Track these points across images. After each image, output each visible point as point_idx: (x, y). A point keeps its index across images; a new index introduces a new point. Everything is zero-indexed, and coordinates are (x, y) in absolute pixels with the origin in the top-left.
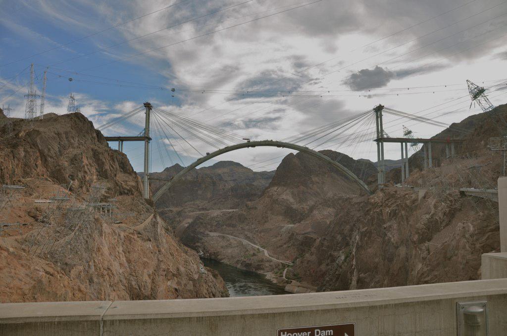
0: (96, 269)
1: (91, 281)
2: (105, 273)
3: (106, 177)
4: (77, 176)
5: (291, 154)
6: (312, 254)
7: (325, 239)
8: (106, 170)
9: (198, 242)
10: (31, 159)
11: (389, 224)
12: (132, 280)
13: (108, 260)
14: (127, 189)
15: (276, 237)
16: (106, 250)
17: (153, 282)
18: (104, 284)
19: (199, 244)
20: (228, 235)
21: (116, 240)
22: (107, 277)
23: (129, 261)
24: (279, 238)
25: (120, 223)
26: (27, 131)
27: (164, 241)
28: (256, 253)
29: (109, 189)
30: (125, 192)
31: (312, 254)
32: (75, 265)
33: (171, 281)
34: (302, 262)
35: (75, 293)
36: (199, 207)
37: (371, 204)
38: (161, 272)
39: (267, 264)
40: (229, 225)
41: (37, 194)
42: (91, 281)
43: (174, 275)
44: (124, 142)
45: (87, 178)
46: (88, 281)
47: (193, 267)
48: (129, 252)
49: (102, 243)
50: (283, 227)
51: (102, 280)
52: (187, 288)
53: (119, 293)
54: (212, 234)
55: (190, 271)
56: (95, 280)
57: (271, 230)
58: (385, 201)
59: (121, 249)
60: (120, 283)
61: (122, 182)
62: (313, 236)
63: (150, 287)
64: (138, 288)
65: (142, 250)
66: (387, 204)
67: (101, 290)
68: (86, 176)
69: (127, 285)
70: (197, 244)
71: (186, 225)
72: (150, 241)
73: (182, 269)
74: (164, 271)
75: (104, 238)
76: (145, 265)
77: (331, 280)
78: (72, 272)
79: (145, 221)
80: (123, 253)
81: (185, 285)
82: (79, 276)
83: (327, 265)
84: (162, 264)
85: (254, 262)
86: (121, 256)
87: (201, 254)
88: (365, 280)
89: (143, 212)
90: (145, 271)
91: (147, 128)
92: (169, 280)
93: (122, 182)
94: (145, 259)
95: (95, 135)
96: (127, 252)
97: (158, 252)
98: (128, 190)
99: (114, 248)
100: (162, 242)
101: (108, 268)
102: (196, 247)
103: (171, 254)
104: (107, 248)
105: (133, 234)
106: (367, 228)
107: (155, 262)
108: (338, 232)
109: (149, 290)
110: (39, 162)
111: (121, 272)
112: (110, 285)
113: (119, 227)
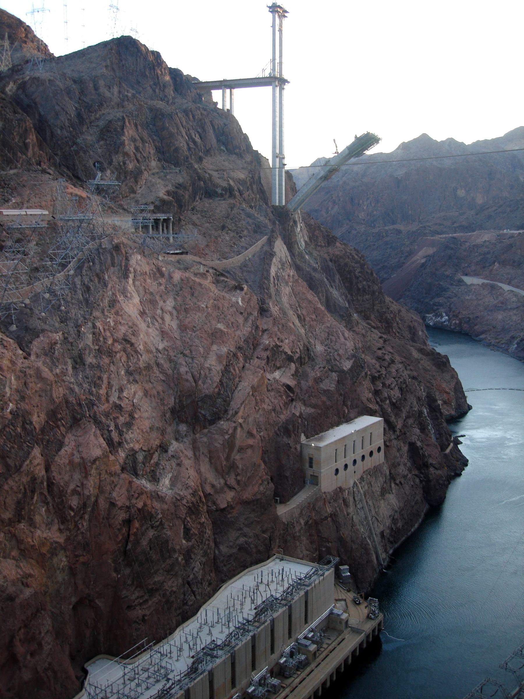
0: (96, 340)
1: (79, 361)
2: (118, 347)
3: (177, 165)
4: (110, 163)
8: (177, 150)
9: (438, 295)
10: (15, 134)
12: (181, 364)
13: (130, 324)
16: (131, 307)
17: (226, 370)
18: (112, 368)
19: (441, 300)
20: (500, 285)
21: (162, 287)
22: (121, 357)
23: (183, 328)
25: (182, 253)
26: (19, 82)
27: (286, 290)
29: (179, 186)
30: (216, 192)
32: (43, 331)
33: (283, 369)
35: (28, 381)
36: (453, 223)
38: (259, 352)
40: (503, 263)
41: (19, 200)
42: (79, 361)
43: (290, 359)
44: (236, 91)
45: (131, 166)
46: (69, 362)
47: (346, 345)
48: (186, 310)
49: (124, 292)
51: (106, 360)
52: (322, 386)
53: (148, 386)
54: (468, 280)
55: (336, 353)
56: (90, 360)
59: (170, 304)
60: (155, 368)
61: (215, 174)
63: (217, 379)
64: (191, 379)
65: (216, 307)
67: (100, 378)
68: (128, 162)
69: (170, 372)
70: (437, 300)
71: (423, 261)
72: (242, 289)
73: (319, 348)
74: (266, 350)
75: (130, 281)
76: (216, 336)
78: (35, 343)
79: (247, 249)
80: (175, 313)
81: (318, 380)
82: (49, 351)
84: (265, 336)
86: (167, 318)
87: (443, 320)
89: (245, 232)
90: (215, 347)
91: (276, 60)
92: (279, 368)
93: (215, 174)
94: (220, 326)
95: (167, 78)
96: (181, 310)
97: (256, 313)
99: (153, 302)
100: (278, 292)
101: (126, 340)
102: (434, 305)
103: (299, 317)
104: (136, 300)
105: (203, 275)
107: (246, 330)
109: (215, 385)
110: (32, 138)
111: (161, 347)
112: (129, 373)
113: (178, 262)
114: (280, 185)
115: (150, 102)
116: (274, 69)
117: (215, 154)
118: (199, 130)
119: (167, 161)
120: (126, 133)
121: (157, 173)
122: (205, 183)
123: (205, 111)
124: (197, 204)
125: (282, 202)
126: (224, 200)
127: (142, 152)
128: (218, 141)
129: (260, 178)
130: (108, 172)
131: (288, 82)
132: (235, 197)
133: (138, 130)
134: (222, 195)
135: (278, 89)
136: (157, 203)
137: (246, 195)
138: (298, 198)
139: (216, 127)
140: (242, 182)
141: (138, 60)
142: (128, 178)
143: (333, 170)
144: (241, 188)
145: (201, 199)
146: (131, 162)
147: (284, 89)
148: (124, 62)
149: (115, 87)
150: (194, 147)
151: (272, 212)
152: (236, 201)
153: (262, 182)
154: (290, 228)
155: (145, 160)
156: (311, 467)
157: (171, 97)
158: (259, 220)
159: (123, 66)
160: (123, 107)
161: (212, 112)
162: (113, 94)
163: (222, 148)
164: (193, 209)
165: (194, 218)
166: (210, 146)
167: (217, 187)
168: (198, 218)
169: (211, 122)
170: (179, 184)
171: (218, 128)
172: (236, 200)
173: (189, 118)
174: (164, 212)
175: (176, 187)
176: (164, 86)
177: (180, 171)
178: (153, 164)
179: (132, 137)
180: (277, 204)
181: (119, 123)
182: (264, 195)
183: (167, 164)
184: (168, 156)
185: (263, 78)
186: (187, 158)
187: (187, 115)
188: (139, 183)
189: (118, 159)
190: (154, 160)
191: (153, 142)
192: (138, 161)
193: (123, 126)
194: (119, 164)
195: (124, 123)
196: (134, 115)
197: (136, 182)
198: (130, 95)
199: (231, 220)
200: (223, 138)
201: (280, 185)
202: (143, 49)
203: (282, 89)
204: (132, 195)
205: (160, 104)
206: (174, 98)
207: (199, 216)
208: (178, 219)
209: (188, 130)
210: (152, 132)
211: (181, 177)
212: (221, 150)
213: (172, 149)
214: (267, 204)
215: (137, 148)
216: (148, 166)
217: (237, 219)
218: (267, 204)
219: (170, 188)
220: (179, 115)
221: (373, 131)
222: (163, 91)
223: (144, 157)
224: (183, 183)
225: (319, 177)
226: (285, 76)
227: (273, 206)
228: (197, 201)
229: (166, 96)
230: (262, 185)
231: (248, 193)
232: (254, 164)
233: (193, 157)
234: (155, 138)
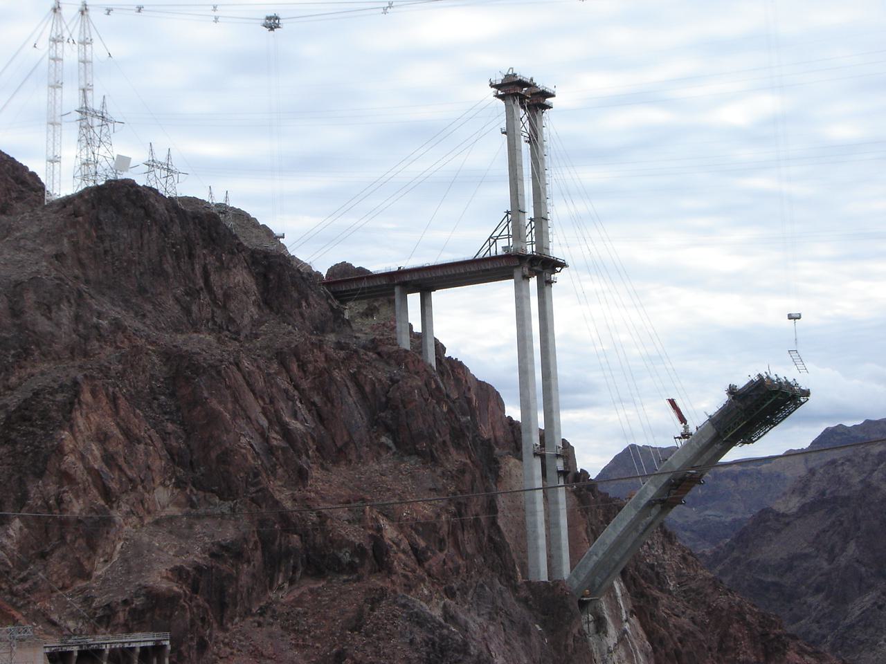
3: (227, 492)
4: (22, 501)
8: (225, 457)
14: (350, 544)
29: (221, 552)
30: (338, 561)
44: (437, 296)
45: (77, 508)
68: (68, 496)
93: (343, 513)
95: (241, 277)
98: (359, 551)
114: (551, 524)
115: (166, 338)
116: (517, 235)
117: (360, 457)
118: (317, 399)
119: (197, 485)
120: (81, 421)
121: (171, 519)
122: (304, 536)
123: (342, 349)
124: (283, 596)
125: (561, 571)
126: (359, 579)
127: (125, 466)
128: (375, 422)
129: (492, 508)
130: (17, 523)
131: (563, 265)
132: (391, 571)
133: (117, 413)
134: (352, 568)
135: (533, 282)
136: (138, 602)
137: (435, 561)
138: (595, 558)
139: (368, 389)
140: (428, 528)
141: (146, 235)
142: (69, 538)
143: (683, 480)
144: (422, 544)
145: (292, 582)
146: (77, 497)
147: (550, 283)
148: (107, 244)
149: (65, 306)
150: (284, 444)
151: (525, 601)
152: (393, 582)
153: (500, 523)
154: (571, 641)
155: (134, 488)
157: (246, 321)
158: (445, 632)
159: (106, 252)
160: (86, 354)
161: (362, 351)
162: (58, 325)
163: (383, 439)
164: (262, 612)
165: (259, 636)
166: (346, 438)
167: (340, 548)
168: (270, 636)
169: (354, 377)
170: (222, 547)
171: (373, 390)
172: (394, 578)
173: (288, 371)
174: (155, 628)
175: (213, 555)
176: (227, 296)
177: (232, 509)
178: (162, 495)
179: (99, 428)
180: (544, 577)
181: (60, 397)
182: (499, 553)
183: (201, 494)
184: (204, 470)
185: (492, 259)
186: (256, 475)
187: (283, 364)
188: (100, 551)
189: (41, 490)
190: (163, 484)
191: (164, 440)
192: (107, 494)
193: (72, 404)
194: (47, 503)
195: (77, 394)
196: (113, 373)
197: (92, 547)
198: (105, 323)
199: (367, 635)
200: (386, 415)
201: (551, 524)
202: (161, 208)
203: (545, 284)
204: (80, 584)
205: (201, 343)
206: (256, 323)
207: (276, 629)
208: (194, 643)
209: (272, 402)
210: (166, 413)
211: (228, 526)
212: (382, 445)
213: (213, 455)
214: (509, 579)
215: (109, 459)
216: (142, 502)
217: (382, 633)
218: (509, 579)
219: (197, 555)
220: (246, 363)
221: (783, 371)
222: (224, 307)
223: (131, 480)
224: (233, 543)
225: (644, 502)
226: (555, 252)
227: (529, 583)
228: (280, 588)
229: (231, 320)
230: (498, 528)
231: (442, 556)
232: (468, 477)
233: (280, 471)
234: (170, 427)
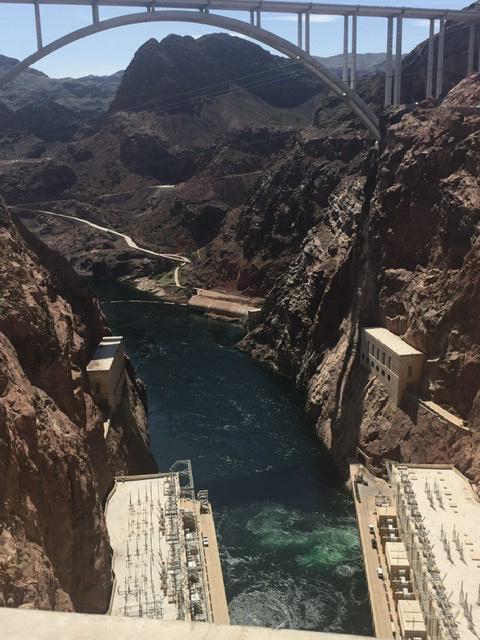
5: (153, 41)
6: (226, 239)
7: (250, 211)
11: (453, 177)
15: (143, 210)
24: (149, 211)
28: (111, 243)
31: (226, 239)
34: (208, 255)
37: (399, 140)
39: (137, 262)
50: (153, 190)
57: (128, 198)
58: (441, 134)
62: (221, 206)
66: (447, 140)
77: (297, 283)
83: (264, 258)
85: (111, 261)
88: (400, 278)
90: (24, 287)
106: (398, 185)
108: (280, 197)
156: (98, 392)
